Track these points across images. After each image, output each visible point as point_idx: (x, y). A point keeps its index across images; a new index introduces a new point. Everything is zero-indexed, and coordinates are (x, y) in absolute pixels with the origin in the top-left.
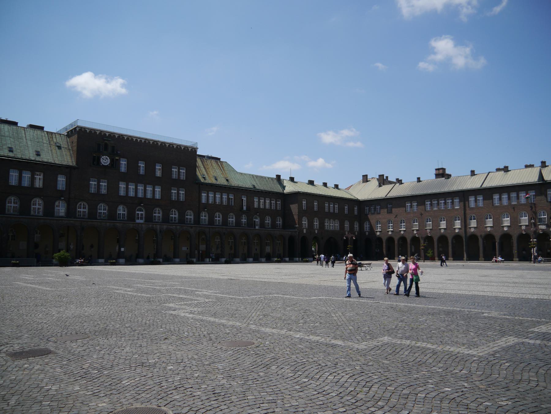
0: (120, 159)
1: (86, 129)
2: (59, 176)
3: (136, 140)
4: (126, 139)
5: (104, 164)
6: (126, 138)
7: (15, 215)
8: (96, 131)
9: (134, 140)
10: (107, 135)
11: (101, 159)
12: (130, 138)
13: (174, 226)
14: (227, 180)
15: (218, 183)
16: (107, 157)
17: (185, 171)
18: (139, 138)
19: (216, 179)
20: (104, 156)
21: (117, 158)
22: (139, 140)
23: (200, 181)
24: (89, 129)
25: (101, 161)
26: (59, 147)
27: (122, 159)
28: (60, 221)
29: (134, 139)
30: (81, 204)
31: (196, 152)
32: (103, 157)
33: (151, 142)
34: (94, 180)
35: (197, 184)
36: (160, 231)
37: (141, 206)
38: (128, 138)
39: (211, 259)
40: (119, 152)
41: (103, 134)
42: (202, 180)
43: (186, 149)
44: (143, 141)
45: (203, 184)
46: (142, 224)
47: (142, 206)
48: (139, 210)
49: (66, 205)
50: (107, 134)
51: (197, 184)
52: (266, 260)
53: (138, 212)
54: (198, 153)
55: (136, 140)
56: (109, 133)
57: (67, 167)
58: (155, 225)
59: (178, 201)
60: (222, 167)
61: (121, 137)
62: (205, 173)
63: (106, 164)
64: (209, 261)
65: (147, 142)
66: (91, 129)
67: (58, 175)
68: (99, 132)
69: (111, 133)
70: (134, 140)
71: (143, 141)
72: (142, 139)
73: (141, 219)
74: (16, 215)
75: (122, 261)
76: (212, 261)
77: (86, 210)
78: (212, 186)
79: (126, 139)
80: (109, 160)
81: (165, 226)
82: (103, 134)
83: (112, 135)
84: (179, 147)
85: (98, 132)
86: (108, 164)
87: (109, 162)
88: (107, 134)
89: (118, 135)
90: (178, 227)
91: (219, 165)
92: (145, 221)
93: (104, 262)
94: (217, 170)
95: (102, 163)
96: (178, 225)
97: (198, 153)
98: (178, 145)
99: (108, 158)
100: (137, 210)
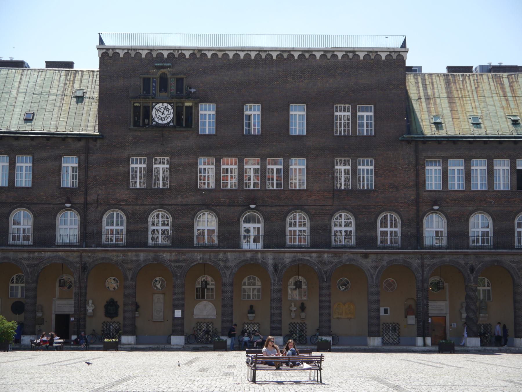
0: (197, 105)
1: (117, 51)
2: (65, 158)
3: (237, 56)
4: (209, 57)
5: (160, 122)
6: (209, 55)
7: (26, 246)
8: (140, 51)
9: (231, 57)
10: (165, 56)
11: (154, 110)
12: (220, 55)
13: (314, 255)
14: (515, 123)
15: (443, 133)
16: (166, 105)
17: (372, 114)
18: (209, 50)
19: (477, 125)
20: (161, 104)
21: (188, 104)
22: (242, 55)
23: (422, 133)
24: (123, 49)
25: (154, 115)
26: (80, 99)
27: (202, 105)
28: (36, 254)
29: (231, 55)
30: (112, 215)
31: (401, 59)
32: (157, 106)
33: (274, 55)
34: (141, 159)
35: (408, 142)
36: (276, 268)
37: (252, 209)
38: (214, 55)
39: (429, 340)
40: (193, 90)
41: (154, 54)
42: (429, 131)
43: (373, 57)
44: (253, 55)
45: (426, 140)
46: (256, 252)
47: (253, 209)
48: (248, 220)
49: (78, 218)
50: (165, 54)
51: (408, 142)
52: (483, 344)
53: (247, 225)
54: (408, 64)
55: (237, 56)
56: (169, 52)
57: (80, 137)
58: (259, 254)
59: (445, 191)
60: (513, 90)
61: (198, 56)
62: (447, 112)
63: (165, 122)
64: (425, 345)
65: (263, 55)
66: (128, 49)
67: (61, 156)
68: (147, 51)
69: (174, 50)
70: (231, 57)
71: (253, 55)
72: (251, 51)
73: (256, 240)
74: (29, 246)
75: (177, 340)
76: (433, 344)
77: (124, 228)
78: (454, 142)
79: (209, 57)
80: (172, 111)
81: (287, 255)
82: (154, 54)
83: (176, 54)
84: (351, 55)
85: (144, 54)
86: (169, 120)
87: (172, 116)
88: (165, 54)
89: (191, 52)
90: (326, 256)
91: (502, 85)
92: (265, 247)
93: (133, 343)
94: (489, 100)
95: (156, 120)
96: (228, 252)
97: (408, 64)
98: (347, 52)
99: (169, 107)
100: (245, 218)
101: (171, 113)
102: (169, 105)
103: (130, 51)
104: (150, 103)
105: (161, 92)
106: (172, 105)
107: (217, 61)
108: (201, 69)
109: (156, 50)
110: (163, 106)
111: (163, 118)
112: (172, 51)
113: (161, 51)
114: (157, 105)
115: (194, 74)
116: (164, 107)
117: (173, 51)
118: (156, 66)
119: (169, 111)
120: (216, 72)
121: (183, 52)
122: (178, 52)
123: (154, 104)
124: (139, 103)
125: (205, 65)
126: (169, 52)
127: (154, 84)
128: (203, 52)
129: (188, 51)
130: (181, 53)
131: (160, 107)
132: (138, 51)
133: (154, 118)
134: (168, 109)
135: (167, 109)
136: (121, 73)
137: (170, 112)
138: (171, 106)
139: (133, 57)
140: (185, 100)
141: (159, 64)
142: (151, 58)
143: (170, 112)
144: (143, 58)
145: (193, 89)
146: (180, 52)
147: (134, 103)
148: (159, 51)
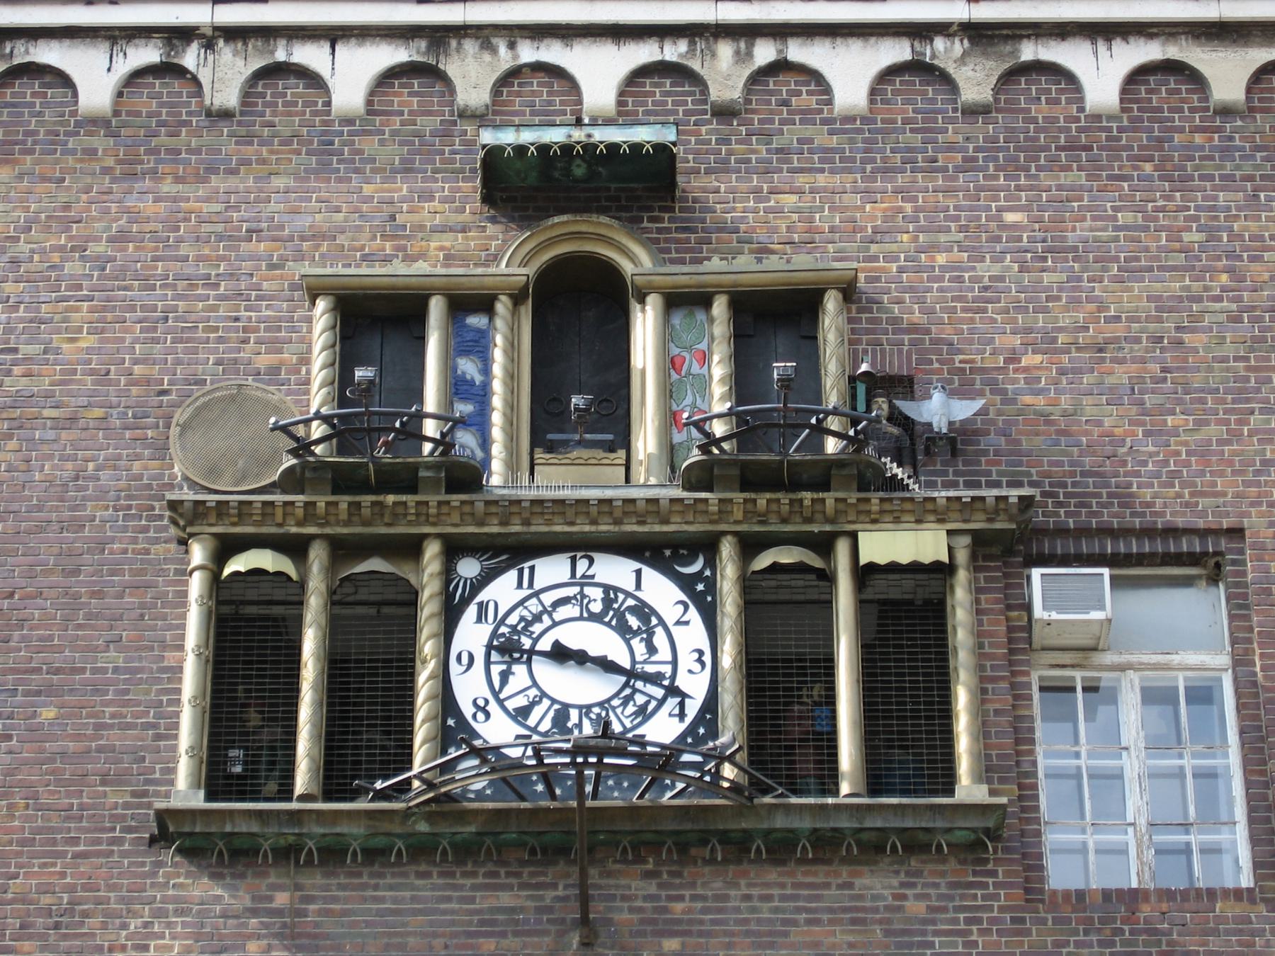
8: (310, 55)
20: (552, 570)
56: (645, 53)
101: (687, 660)
102: (649, 574)
103: (190, 58)
104: (411, 549)
105: (551, 448)
106: (698, 576)
107: (1198, 139)
108: (1010, 217)
109: (488, 46)
110: (588, 580)
111: (585, 709)
112: (673, 51)
113: (553, 53)
114: (512, 575)
115: (941, 259)
116: (596, 593)
117: (683, 46)
118: (493, 156)
119: (660, 638)
120: (1193, 237)
121: (797, 52)
122: (743, 57)
123: (469, 568)
124: (295, 548)
125: (1065, 178)
126: (645, 53)
127: (468, 367)
128: (1029, 51)
129: (856, 45)
130: (780, 67)
131: (548, 598)
132: (281, 56)
133: (468, 710)
134: (644, 611)
135: (633, 622)
136: (73, 267)
137: (664, 653)
138: (686, 583)
139: (226, 114)
140: (853, 497)
141: (527, 137)
142: (428, 124)
143: (664, 653)
144: (348, 121)
145: (937, 397)
146: (765, 53)
147: (226, 548)
148: (528, 53)
